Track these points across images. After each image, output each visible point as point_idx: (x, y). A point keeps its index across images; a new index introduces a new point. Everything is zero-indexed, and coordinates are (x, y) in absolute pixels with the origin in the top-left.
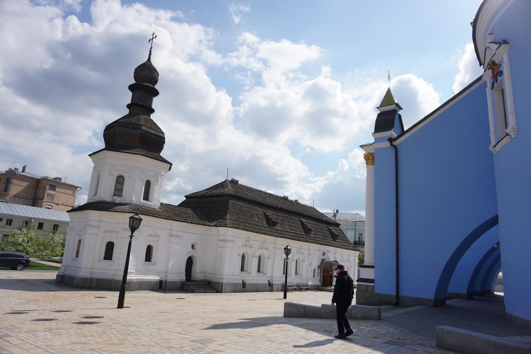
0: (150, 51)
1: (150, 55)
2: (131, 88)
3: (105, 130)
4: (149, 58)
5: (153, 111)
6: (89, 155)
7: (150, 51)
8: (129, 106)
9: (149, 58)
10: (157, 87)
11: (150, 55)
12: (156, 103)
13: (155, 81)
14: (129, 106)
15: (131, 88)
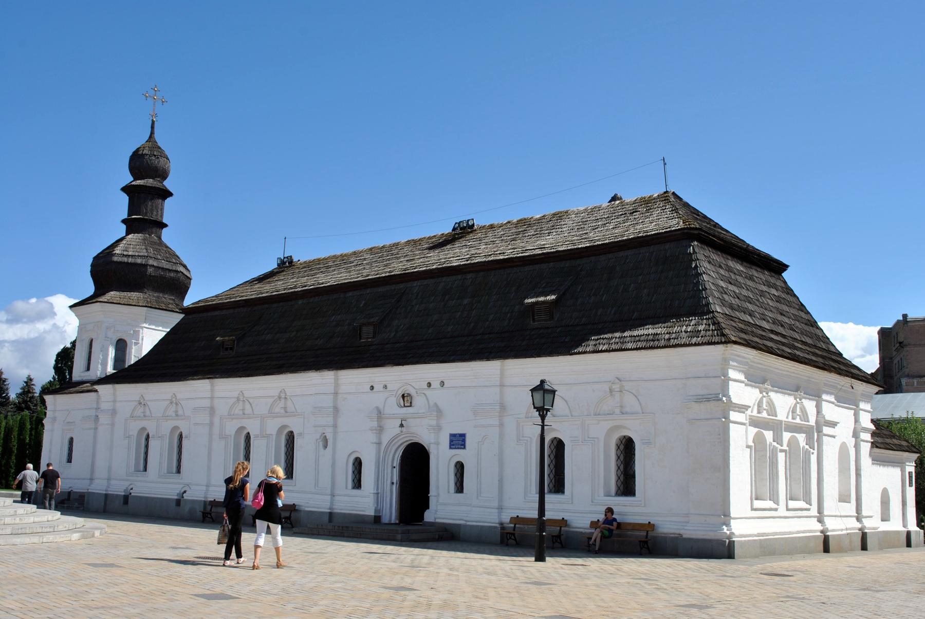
0: (153, 122)
1: (153, 127)
2: (126, 189)
3: (92, 265)
4: (152, 133)
5: (166, 226)
6: (71, 307)
7: (153, 122)
8: (124, 221)
9: (152, 133)
10: (168, 184)
11: (153, 127)
12: (170, 210)
13: (163, 174)
14: (124, 221)
15: (126, 189)
